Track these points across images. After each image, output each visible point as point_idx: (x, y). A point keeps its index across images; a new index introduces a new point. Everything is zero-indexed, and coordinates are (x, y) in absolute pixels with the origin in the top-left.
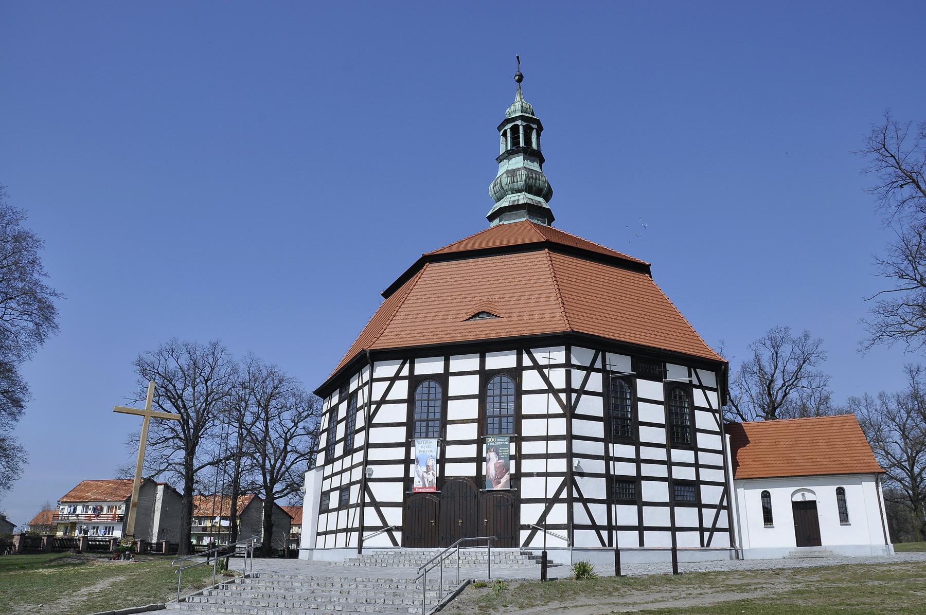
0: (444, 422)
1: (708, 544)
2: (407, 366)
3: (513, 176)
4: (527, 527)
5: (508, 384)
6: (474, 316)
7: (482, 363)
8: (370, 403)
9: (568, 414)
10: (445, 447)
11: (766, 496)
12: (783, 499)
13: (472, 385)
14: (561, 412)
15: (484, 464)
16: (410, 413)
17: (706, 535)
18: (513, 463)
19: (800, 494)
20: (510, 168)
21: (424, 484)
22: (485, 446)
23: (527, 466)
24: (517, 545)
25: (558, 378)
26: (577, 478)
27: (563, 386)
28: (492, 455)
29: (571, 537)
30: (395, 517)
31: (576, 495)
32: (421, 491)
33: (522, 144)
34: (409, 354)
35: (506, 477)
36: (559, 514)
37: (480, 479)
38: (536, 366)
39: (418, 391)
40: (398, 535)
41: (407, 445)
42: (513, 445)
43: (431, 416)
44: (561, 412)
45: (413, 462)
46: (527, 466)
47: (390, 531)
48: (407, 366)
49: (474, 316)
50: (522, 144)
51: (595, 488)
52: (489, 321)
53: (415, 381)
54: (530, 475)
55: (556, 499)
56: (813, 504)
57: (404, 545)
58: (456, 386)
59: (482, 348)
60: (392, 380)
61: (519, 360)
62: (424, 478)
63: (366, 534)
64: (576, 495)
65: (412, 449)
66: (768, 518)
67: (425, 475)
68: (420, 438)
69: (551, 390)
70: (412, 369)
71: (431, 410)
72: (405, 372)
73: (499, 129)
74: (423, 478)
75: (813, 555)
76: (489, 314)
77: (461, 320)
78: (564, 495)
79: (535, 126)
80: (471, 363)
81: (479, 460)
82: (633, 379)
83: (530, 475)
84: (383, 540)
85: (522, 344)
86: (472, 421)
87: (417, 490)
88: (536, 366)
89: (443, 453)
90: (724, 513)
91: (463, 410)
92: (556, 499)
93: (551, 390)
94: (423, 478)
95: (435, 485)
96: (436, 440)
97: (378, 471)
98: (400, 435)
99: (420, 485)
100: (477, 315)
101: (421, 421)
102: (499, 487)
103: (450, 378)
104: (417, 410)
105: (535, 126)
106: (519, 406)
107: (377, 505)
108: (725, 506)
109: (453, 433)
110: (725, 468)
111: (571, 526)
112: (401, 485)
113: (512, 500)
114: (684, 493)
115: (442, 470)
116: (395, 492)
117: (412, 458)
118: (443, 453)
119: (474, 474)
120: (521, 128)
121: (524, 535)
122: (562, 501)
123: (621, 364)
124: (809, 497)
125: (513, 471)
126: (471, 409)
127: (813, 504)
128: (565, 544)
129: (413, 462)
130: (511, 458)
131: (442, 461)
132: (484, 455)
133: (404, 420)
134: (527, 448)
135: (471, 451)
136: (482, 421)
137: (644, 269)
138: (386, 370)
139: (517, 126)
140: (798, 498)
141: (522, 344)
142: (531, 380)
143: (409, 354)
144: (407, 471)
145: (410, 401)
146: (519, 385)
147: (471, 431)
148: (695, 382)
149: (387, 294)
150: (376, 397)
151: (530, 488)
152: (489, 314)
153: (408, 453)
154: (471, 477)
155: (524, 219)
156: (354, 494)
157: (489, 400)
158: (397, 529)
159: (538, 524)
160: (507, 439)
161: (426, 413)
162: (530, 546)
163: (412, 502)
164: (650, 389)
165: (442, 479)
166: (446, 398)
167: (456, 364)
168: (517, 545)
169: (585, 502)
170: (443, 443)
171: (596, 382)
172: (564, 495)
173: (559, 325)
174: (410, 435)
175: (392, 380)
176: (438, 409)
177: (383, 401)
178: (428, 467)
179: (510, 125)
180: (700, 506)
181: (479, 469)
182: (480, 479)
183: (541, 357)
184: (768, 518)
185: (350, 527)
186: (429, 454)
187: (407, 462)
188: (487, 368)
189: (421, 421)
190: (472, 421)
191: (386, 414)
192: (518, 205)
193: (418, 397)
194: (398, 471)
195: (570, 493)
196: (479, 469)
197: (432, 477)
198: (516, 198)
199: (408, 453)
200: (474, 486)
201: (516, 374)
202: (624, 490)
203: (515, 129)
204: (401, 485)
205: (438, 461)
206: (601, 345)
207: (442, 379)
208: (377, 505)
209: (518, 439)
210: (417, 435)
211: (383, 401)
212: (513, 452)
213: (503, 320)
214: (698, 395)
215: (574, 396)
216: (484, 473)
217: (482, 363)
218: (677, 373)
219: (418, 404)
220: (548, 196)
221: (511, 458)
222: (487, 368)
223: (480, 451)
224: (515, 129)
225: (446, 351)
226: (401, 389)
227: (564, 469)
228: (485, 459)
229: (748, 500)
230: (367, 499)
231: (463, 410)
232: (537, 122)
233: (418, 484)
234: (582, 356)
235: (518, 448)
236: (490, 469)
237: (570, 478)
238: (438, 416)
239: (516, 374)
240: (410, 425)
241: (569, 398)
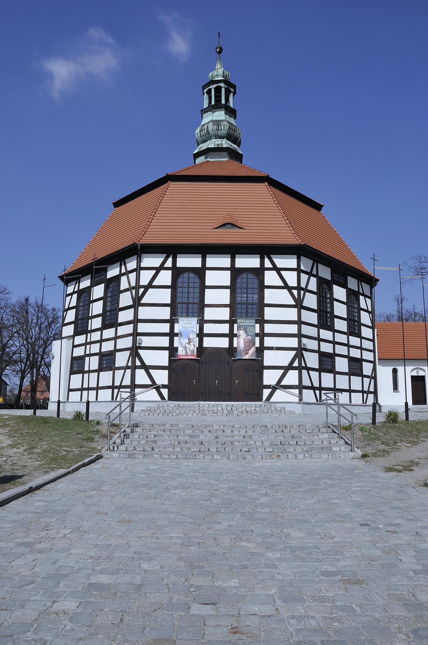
0: (202, 306)
1: (366, 403)
2: (170, 260)
3: (218, 125)
4: (268, 387)
5: (253, 280)
6: (222, 226)
7: (233, 262)
8: (138, 286)
9: (299, 306)
10: (203, 324)
11: (395, 371)
12: (406, 373)
13: (225, 278)
14: (294, 303)
15: (235, 339)
16: (173, 296)
17: (365, 395)
18: (257, 339)
19: (415, 371)
20: (215, 119)
21: (186, 352)
22: (235, 326)
23: (268, 342)
24: (261, 400)
25: (291, 278)
26: (304, 352)
27: (296, 285)
28: (242, 332)
29: (300, 393)
30: (162, 377)
31: (303, 365)
32: (184, 357)
33: (223, 102)
34: (172, 250)
35: (253, 350)
36: (292, 378)
37: (231, 350)
38: (275, 268)
39: (180, 280)
40: (165, 392)
41: (172, 322)
42: (257, 326)
43: (191, 300)
44: (294, 303)
45: (177, 335)
46: (268, 342)
47: (158, 389)
48: (170, 260)
49: (222, 226)
50: (223, 102)
51: (312, 360)
52: (235, 230)
53: (177, 272)
54: (271, 348)
55: (290, 367)
56: (422, 378)
57: (170, 399)
58: (211, 278)
59: (233, 250)
60: (158, 270)
61: (262, 263)
62: (186, 348)
63: (137, 390)
64: (303, 365)
65: (176, 325)
66: (395, 387)
67: (187, 345)
68: (182, 316)
69: (286, 286)
70: (174, 262)
71: (191, 295)
72: (169, 263)
73: (204, 87)
74: (185, 348)
75: (423, 410)
76: (233, 225)
77: (214, 227)
78: (296, 364)
79: (232, 90)
80: (224, 261)
81: (231, 336)
82: (332, 284)
83: (271, 348)
84: (153, 395)
85: (265, 251)
86: (225, 306)
87: (181, 357)
88: (275, 268)
89: (201, 329)
90: (373, 380)
91: (217, 297)
92: (290, 367)
93: (286, 286)
94: (185, 348)
95: (195, 354)
96: (196, 319)
97: (146, 341)
98: (166, 313)
99: (183, 353)
100: (224, 225)
101: (182, 303)
102: (247, 357)
103: (207, 272)
104: (179, 295)
105: (232, 90)
106: (262, 297)
107: (147, 368)
108: (374, 377)
109: (209, 314)
110: (373, 351)
111: (301, 387)
112: (166, 353)
113: (257, 366)
114: (355, 367)
115: (201, 342)
116: (163, 358)
117: (176, 331)
118: (201, 329)
119: (227, 346)
120: (223, 89)
121: (266, 392)
122: (295, 368)
123: (325, 272)
124: (421, 373)
125: (257, 345)
126: (224, 296)
127: (422, 378)
128: (297, 400)
129: (177, 335)
130: (257, 335)
131: (201, 335)
132: (235, 332)
133: (169, 302)
134: (268, 328)
135: (225, 329)
136: (232, 306)
137: (318, 207)
138: (152, 261)
139: (221, 87)
140: (415, 374)
141: (265, 251)
142: (271, 278)
143: (172, 250)
144: (171, 342)
145: (173, 287)
146: (263, 281)
147: (224, 314)
148: (361, 291)
149: (117, 204)
150: (144, 281)
151: (269, 358)
152: (233, 225)
153: (172, 328)
154: (225, 349)
155: (226, 159)
156: (122, 359)
157: (238, 290)
158: (164, 386)
159: (276, 385)
160: (254, 321)
161: (188, 297)
162: (271, 400)
163: (175, 365)
164: (339, 293)
165: (201, 349)
166: (203, 287)
167: (212, 261)
168: (261, 400)
169: (308, 369)
170: (202, 322)
171: (313, 285)
172: (296, 364)
173: (292, 240)
174: (173, 313)
175: (158, 270)
176: (197, 295)
177: (150, 286)
178: (189, 339)
179: (215, 86)
180: (363, 376)
181: (231, 342)
182: (231, 350)
183: (281, 262)
184: (395, 387)
185: (117, 383)
186: (190, 329)
187: (172, 335)
188: (237, 266)
189: (182, 303)
190: (225, 306)
191: (152, 296)
192: (222, 148)
193: (179, 285)
194: (165, 342)
195: (300, 363)
196: (231, 342)
197: (193, 347)
198: (220, 142)
199: (172, 328)
200: (227, 355)
201: (259, 273)
202: (327, 363)
203: (218, 90)
204: (166, 353)
205: (198, 335)
206: (318, 257)
207: (200, 272)
208: (147, 368)
209: (262, 322)
210: (179, 314)
211: (150, 286)
212: (257, 331)
213: (245, 231)
214: (362, 298)
215: (302, 292)
216: (235, 345)
217: (233, 262)
218: (352, 283)
219: (179, 290)
220: (239, 145)
221: (257, 335)
222: (237, 266)
223: (231, 329)
224: (218, 90)
225: (204, 250)
226: (165, 277)
227: (296, 346)
228: (236, 335)
229: (384, 373)
230: (138, 363)
231: (217, 297)
232: (234, 87)
233: (181, 352)
234: (306, 264)
235: (262, 328)
236: (240, 342)
237: (300, 351)
238: (196, 300)
239: (259, 273)
240: (173, 306)
241: (299, 294)
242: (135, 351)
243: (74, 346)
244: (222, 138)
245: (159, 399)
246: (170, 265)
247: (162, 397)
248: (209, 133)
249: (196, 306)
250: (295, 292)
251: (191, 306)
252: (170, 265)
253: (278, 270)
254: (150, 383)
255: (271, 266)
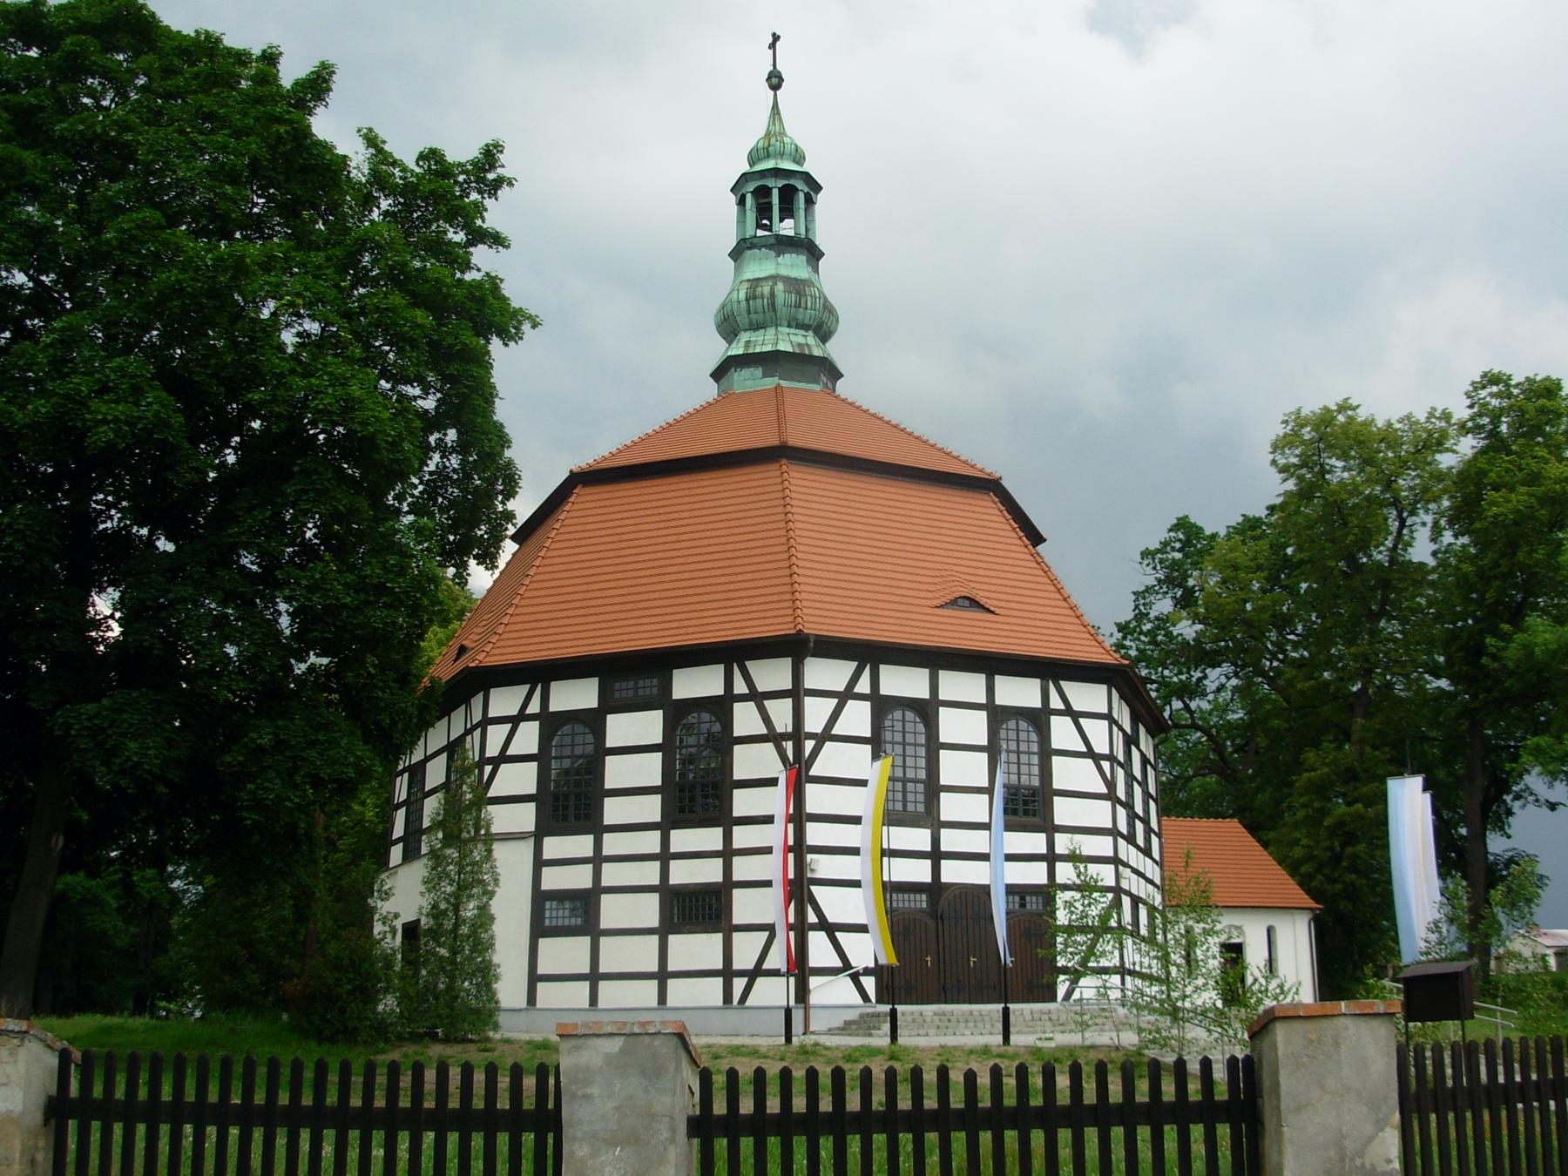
6: (953, 603)
13: (974, 727)
24: (1053, 999)
25: (1098, 734)
34: (870, 654)
38: (1069, 711)
40: (869, 983)
47: (855, 978)
72: (863, 686)
88: (1069, 711)
93: (1090, 753)
106: (1046, 773)
138: (826, 674)
143: (870, 654)
168: (1053, 999)
176: (922, 763)
177: (826, 736)
211: (826, 736)
225: (936, 659)
226: (857, 718)
230: (812, 918)
238: (922, 775)
242: (799, 890)
243: (539, 863)
244: (805, 327)
245: (860, 1001)
246: (868, 691)
247: (865, 997)
248: (774, 310)
249: (921, 787)
250: (1106, 765)
251: (910, 786)
252: (868, 691)
253: (1075, 716)
254: (838, 964)
255: (1062, 707)
